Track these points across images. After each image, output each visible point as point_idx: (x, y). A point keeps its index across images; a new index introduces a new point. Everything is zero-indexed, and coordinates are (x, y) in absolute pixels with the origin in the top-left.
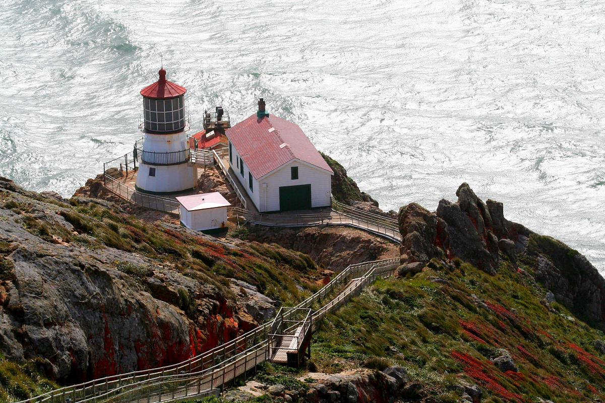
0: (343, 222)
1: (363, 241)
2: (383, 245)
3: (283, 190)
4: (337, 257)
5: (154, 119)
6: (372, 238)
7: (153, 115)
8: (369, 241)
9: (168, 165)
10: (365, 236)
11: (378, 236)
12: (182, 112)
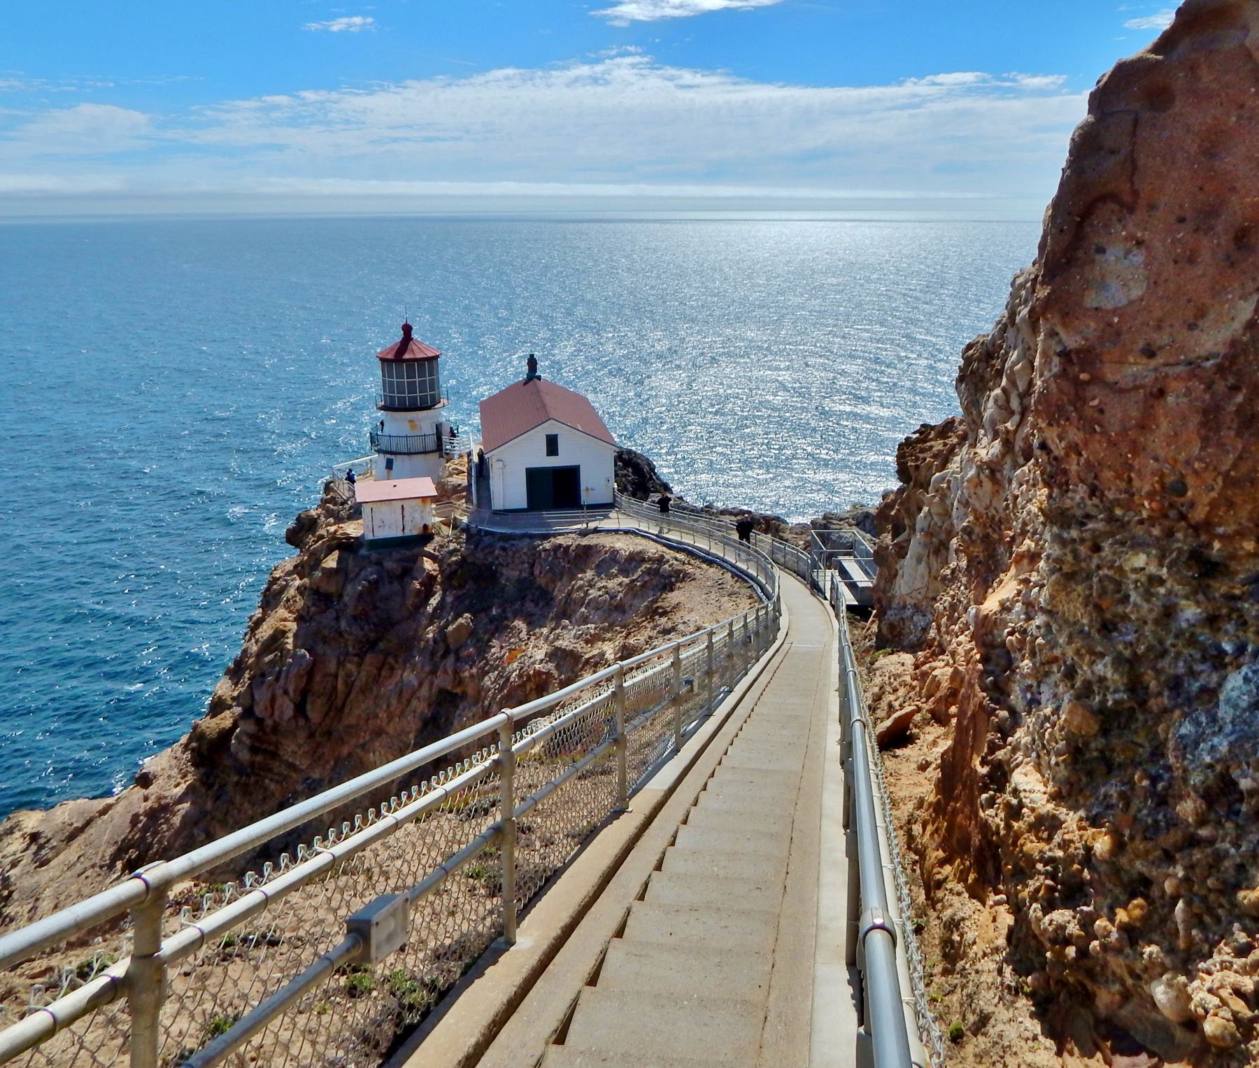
0: (623, 527)
1: (650, 559)
2: (686, 567)
3: (534, 476)
4: (599, 589)
5: (392, 391)
6: (669, 554)
7: (391, 383)
8: (661, 560)
9: (409, 454)
10: (653, 549)
11: (679, 550)
12: (434, 385)
